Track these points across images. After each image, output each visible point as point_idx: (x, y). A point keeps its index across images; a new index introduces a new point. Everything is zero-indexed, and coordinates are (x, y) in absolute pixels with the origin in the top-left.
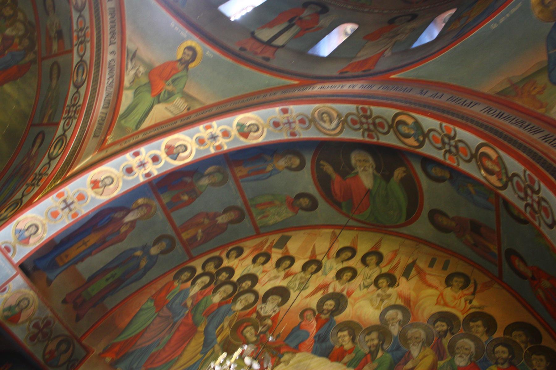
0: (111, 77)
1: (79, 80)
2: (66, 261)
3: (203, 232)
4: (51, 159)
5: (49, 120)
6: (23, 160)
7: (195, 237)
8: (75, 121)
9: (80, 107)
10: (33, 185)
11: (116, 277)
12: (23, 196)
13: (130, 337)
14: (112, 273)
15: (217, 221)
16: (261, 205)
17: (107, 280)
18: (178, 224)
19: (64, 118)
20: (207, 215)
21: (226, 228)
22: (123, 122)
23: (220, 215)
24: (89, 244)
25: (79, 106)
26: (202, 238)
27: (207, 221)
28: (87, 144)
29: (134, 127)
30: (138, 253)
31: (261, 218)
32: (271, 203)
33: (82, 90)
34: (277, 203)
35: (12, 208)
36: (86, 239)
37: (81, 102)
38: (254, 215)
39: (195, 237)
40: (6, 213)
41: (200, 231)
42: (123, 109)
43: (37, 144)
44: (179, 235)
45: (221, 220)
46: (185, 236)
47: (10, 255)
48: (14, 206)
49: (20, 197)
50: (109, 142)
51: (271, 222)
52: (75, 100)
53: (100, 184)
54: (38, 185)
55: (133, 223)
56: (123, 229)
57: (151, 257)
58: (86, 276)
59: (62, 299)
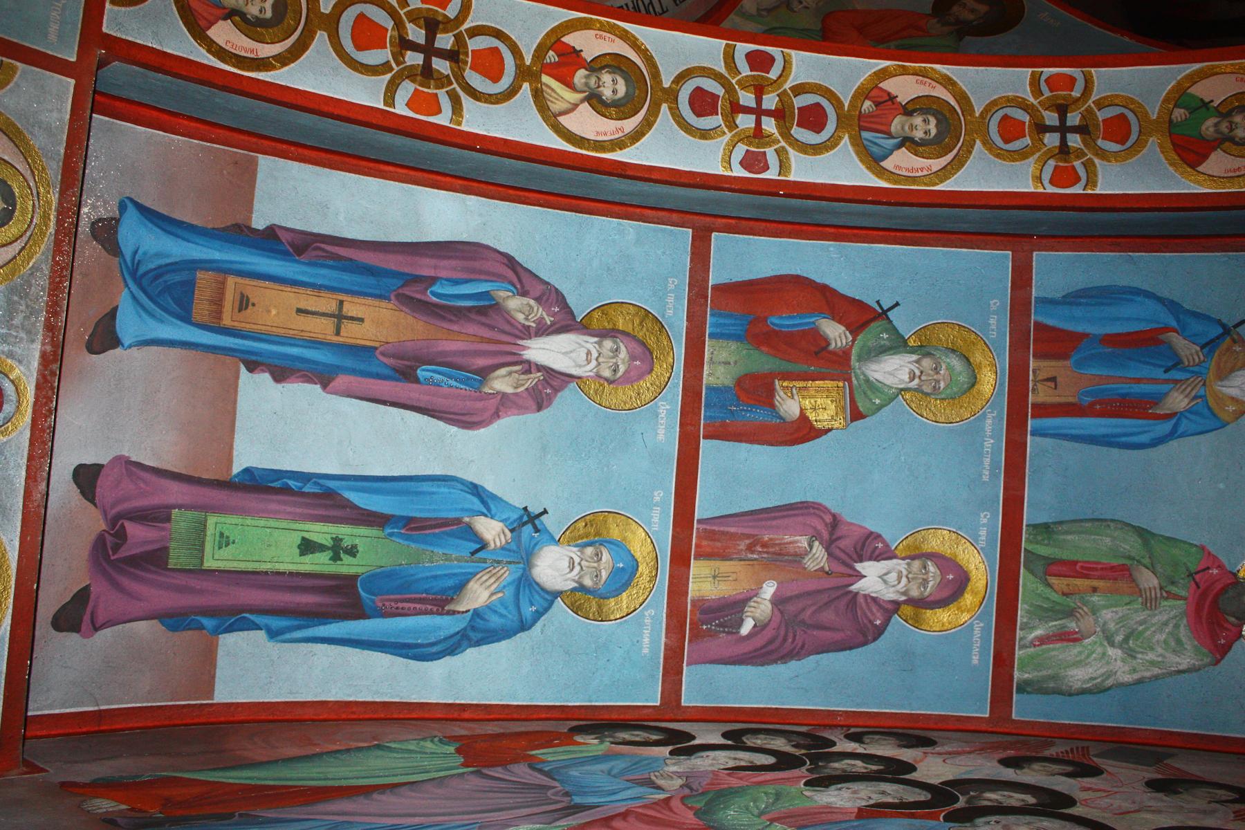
2: (227, 321)
3: (777, 601)
7: (732, 609)
11: (347, 566)
13: (300, 783)
14: (347, 532)
15: (861, 577)
16: (1071, 569)
17: (307, 547)
18: (703, 508)
20: (831, 528)
21: (879, 631)
23: (886, 554)
24: (351, 333)
26: (758, 629)
27: (818, 557)
30: (491, 529)
31: (1042, 640)
32: (1117, 574)
34: (1148, 580)
36: (353, 307)
38: (1021, 617)
39: (732, 609)
41: (769, 589)
44: (680, 559)
45: (875, 579)
46: (705, 581)
51: (1078, 676)
53: (580, 76)
55: (554, 380)
56: (502, 382)
57: (526, 582)
58: (249, 454)
59: (89, 460)
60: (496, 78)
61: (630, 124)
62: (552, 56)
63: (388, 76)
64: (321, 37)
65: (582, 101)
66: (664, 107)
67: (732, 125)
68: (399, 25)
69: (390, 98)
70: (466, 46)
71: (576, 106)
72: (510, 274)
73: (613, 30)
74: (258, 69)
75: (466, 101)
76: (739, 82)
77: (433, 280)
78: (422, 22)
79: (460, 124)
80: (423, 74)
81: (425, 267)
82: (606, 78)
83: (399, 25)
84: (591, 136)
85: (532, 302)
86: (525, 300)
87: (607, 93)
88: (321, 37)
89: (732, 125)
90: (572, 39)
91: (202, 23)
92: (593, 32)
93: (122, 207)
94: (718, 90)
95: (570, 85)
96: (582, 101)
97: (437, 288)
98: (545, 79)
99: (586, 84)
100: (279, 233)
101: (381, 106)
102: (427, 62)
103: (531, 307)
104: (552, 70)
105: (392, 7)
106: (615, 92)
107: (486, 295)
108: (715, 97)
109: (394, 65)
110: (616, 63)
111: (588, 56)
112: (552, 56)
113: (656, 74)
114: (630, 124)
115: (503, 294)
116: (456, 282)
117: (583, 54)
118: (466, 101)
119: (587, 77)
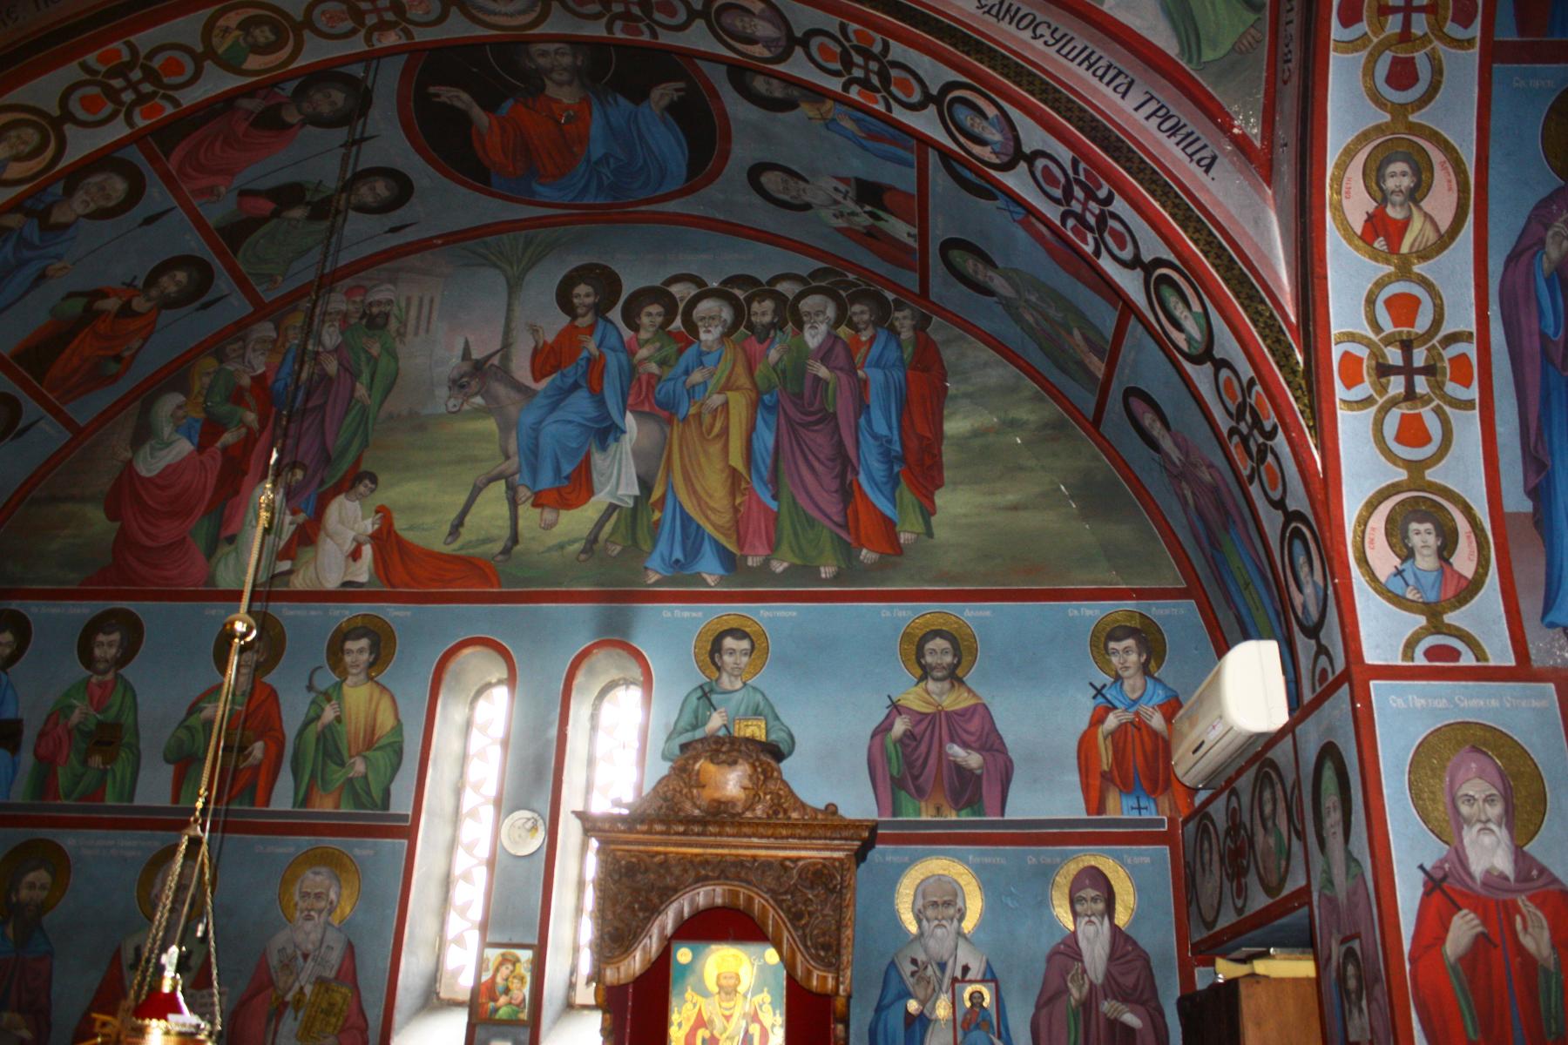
0: (1034, 25)
1: (995, 136)
4: (1205, 355)
5: (1099, 352)
6: (1185, 504)
8: (1119, 206)
9: (1082, 165)
10: (1263, 451)
12: (1279, 505)
19: (1097, 253)
22: (1208, 55)
25: (1075, 164)
28: (1218, 204)
29: (1251, 17)
33: (1033, 136)
35: (1301, 560)
37: (1065, 155)
40: (1309, 590)
42: (1164, 39)
43: (1157, 430)
47: (1467, 660)
48: (1298, 544)
49: (1279, 516)
50: (1255, 131)
52: (1053, 181)
53: (1394, 213)
54: (1271, 435)
60: (1415, 302)
61: (1436, 156)
62: (1380, 243)
63: (1447, 409)
64: (1431, 475)
65: (1420, 209)
66: (1413, 118)
67: (1424, 40)
68: (1394, 402)
69: (1467, 405)
70: (1392, 334)
71: (1427, 216)
72: (1525, 258)
73: (1338, 180)
74: (1483, 530)
75: (1446, 329)
76: (1375, 34)
77: (1543, 335)
78: (1383, 380)
79: (1471, 334)
80: (1434, 375)
81: (1532, 346)
82: (1390, 184)
83: (1394, 402)
84: (1454, 196)
85: (1550, 233)
86: (1549, 240)
87: (1406, 182)
88: (1431, 475)
89: (1424, 40)
90: (1358, 225)
91: (1464, 584)
92: (1345, 202)
93: (1552, 625)
94: (1387, 57)
95: (1405, 225)
96: (1420, 209)
97: (1550, 331)
98: (1405, 249)
99: (1402, 205)
100: (1533, 482)
101: (1477, 412)
102: (1421, 371)
103: (1556, 234)
104: (1394, 247)
105: (1379, 411)
106: (1404, 174)
107: (1549, 281)
108: (1395, 61)
109: (1433, 404)
110: (1374, 175)
111: (1371, 206)
112: (1380, 243)
113: (1379, 129)
114: (1436, 156)
115: (1546, 265)
116: (1541, 314)
117: (1371, 210)
118: (1446, 329)
119: (1394, 205)
